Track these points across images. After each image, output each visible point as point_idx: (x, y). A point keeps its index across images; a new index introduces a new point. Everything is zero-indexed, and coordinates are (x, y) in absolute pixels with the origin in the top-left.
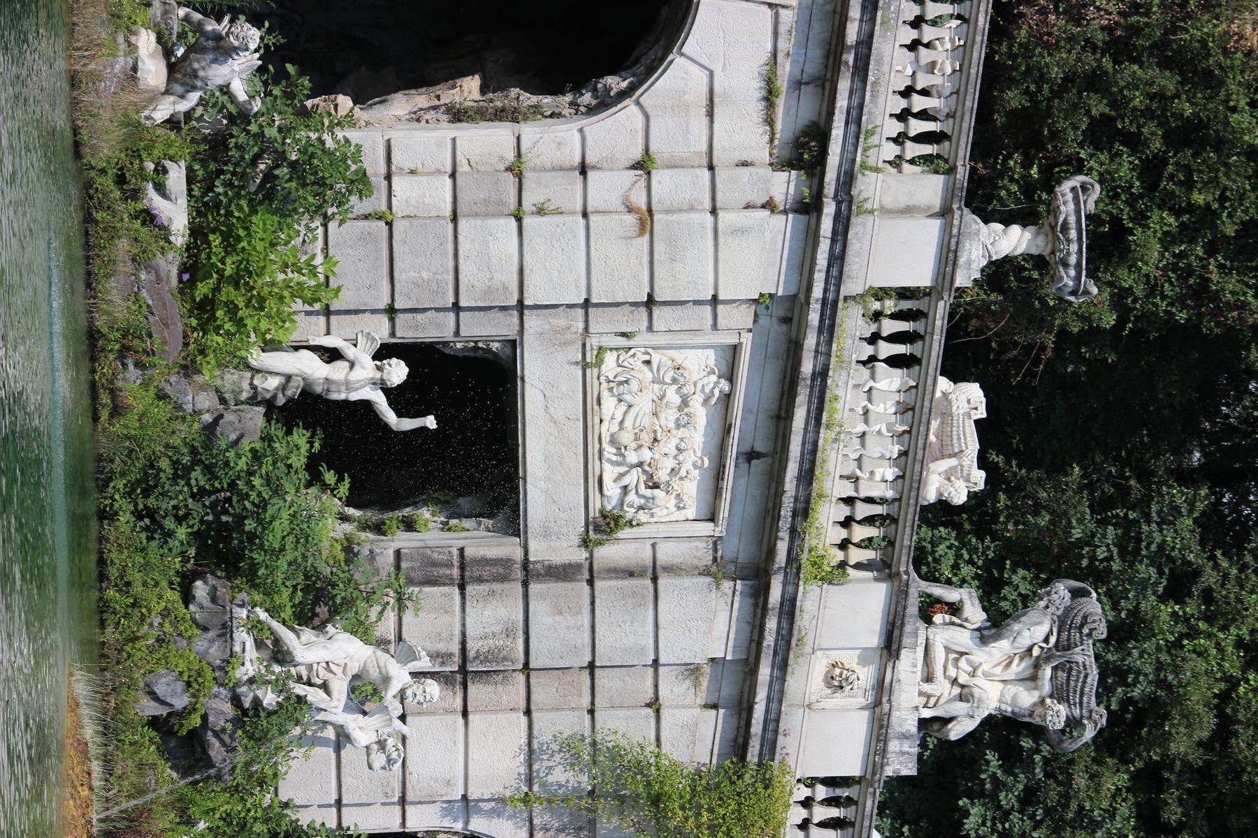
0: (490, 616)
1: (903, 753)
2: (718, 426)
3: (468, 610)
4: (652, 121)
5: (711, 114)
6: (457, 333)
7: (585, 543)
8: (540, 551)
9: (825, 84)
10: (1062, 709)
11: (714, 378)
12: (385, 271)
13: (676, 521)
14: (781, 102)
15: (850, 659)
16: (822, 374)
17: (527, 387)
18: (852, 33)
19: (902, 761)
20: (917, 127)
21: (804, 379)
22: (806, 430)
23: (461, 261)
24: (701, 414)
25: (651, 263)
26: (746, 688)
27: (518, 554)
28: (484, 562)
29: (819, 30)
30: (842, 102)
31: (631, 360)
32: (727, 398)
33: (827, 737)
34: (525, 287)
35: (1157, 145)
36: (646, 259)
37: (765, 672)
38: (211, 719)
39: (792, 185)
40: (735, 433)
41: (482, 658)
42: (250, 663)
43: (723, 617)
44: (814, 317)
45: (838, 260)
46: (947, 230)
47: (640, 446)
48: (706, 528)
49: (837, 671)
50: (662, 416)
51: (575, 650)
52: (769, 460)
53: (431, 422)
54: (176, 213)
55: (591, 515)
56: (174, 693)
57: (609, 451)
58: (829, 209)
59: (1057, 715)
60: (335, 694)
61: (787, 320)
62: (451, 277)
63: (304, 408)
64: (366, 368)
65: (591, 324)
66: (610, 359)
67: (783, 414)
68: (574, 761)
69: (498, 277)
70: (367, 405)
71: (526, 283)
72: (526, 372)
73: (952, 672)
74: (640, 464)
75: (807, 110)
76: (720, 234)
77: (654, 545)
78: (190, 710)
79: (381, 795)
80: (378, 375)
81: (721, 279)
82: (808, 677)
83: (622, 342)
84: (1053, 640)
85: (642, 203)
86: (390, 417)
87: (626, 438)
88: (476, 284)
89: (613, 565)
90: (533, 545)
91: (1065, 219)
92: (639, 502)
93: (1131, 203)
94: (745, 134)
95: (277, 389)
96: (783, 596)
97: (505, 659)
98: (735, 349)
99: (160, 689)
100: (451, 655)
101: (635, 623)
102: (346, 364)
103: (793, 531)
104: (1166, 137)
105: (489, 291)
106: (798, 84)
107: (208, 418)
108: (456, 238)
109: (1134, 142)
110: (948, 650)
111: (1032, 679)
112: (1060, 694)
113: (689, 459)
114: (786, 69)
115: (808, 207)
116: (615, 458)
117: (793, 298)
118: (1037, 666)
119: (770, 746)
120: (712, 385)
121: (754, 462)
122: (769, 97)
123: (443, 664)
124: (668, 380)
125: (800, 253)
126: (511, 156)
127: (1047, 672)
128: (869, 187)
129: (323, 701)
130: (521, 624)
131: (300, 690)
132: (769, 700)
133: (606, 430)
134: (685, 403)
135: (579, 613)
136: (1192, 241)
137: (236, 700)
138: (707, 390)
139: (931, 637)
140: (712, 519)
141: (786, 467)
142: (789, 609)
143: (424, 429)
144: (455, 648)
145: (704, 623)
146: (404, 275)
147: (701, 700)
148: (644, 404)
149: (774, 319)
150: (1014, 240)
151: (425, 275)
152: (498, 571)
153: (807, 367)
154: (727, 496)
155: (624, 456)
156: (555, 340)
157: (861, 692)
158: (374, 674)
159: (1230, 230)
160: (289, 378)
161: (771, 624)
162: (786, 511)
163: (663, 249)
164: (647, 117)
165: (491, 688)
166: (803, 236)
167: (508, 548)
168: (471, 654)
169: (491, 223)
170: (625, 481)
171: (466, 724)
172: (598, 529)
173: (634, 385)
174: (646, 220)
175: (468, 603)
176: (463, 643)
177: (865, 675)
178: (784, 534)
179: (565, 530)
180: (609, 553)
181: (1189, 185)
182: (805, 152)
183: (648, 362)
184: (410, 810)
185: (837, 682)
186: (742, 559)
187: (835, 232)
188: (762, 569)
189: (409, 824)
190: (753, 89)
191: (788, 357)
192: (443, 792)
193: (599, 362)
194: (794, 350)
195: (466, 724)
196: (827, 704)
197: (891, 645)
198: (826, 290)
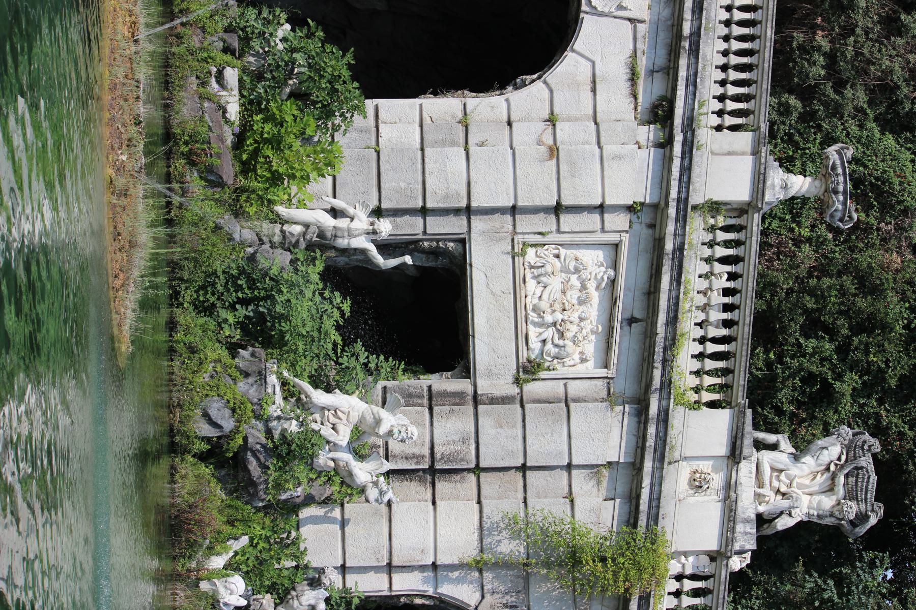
0: (451, 429)
1: (746, 533)
2: (607, 304)
3: (435, 424)
4: (555, 94)
5: (594, 90)
6: (425, 232)
7: (517, 381)
8: (485, 386)
9: (670, 71)
10: (853, 504)
11: (603, 269)
12: (375, 182)
13: (581, 359)
14: (641, 83)
15: (706, 466)
16: (680, 250)
17: (474, 269)
18: (687, 29)
19: (746, 538)
20: (731, 106)
21: (668, 254)
22: (670, 289)
23: (427, 175)
24: (595, 297)
25: (558, 179)
26: (635, 481)
27: (470, 389)
28: (445, 394)
29: (664, 37)
30: (682, 73)
31: (546, 252)
32: (613, 282)
33: (693, 526)
34: (472, 194)
35: (845, 331)
36: (554, 176)
37: (648, 465)
38: (250, 440)
39: (651, 134)
40: (620, 303)
41: (445, 459)
42: (277, 405)
43: (616, 432)
44: (672, 211)
45: (687, 169)
46: (757, 163)
47: (554, 311)
48: (603, 372)
49: (698, 475)
50: (568, 293)
51: (512, 454)
52: (644, 324)
53: (408, 259)
54: (234, 110)
55: (521, 361)
56: (223, 418)
57: (533, 316)
58: (679, 138)
59: (852, 509)
60: (341, 432)
61: (652, 226)
62: (420, 187)
63: (321, 243)
64: (362, 222)
65: (517, 226)
66: (531, 252)
67: (652, 289)
68: (515, 535)
69: (453, 186)
70: (363, 252)
71: (472, 191)
72: (473, 260)
73: (776, 484)
74: (554, 324)
75: (659, 88)
76: (605, 159)
77: (565, 385)
78: (236, 431)
79: (374, 560)
80: (371, 228)
81: (606, 190)
82: (678, 479)
83: (539, 239)
84: (844, 458)
85: (551, 142)
86: (379, 260)
87: (544, 305)
88: (438, 191)
89: (538, 397)
90: (480, 382)
91: (834, 162)
92: (554, 351)
93: (833, 368)
94: (618, 104)
95: (299, 235)
96: (659, 410)
97: (462, 460)
98: (617, 246)
99: (213, 413)
100: (423, 457)
101: (555, 435)
102: (349, 219)
103: (665, 361)
104: (850, 328)
105: (447, 197)
106: (651, 72)
107: (250, 250)
108: (423, 160)
109: (831, 332)
110: (773, 469)
111: (831, 489)
112: (851, 495)
113: (588, 326)
114: (643, 63)
115: (665, 144)
116: (536, 320)
117: (655, 207)
118: (833, 477)
119: (654, 517)
120: (602, 274)
121: (633, 325)
122: (633, 79)
123: (417, 463)
124: (572, 268)
125: (660, 174)
126: (460, 115)
127: (842, 479)
128: (704, 135)
129: (332, 435)
130: (473, 435)
131: (315, 427)
132: (652, 484)
133: (531, 302)
134: (584, 287)
135: (514, 426)
136: (869, 397)
137: (269, 432)
138: (599, 277)
139: (760, 458)
140: (606, 366)
141: (656, 323)
142: (664, 418)
143: (404, 264)
144: (427, 452)
145: (604, 436)
146: (387, 185)
147: (603, 493)
148: (555, 284)
149: (643, 225)
150: (800, 184)
151: (402, 185)
152: (457, 398)
153: (669, 246)
154: (615, 348)
155: (543, 317)
156: (493, 236)
157: (715, 492)
158: (370, 419)
159: (893, 383)
160: (307, 226)
161: (652, 430)
162: (659, 349)
163: (566, 169)
164: (551, 91)
165: (452, 485)
166: (661, 163)
167: (464, 385)
168: (438, 456)
169: (448, 150)
170: (543, 337)
171: (435, 509)
172: (526, 371)
173: (549, 268)
174: (554, 152)
175: (435, 419)
176: (432, 448)
177: (717, 480)
178: (658, 365)
179: (502, 372)
180: (533, 388)
181: (867, 353)
182: (660, 114)
183: (557, 256)
184: (395, 577)
185: (698, 484)
186: (629, 393)
187: (683, 153)
188: (643, 399)
189: (394, 588)
190: (623, 73)
191: (654, 251)
192: (419, 558)
193: (523, 254)
194: (659, 243)
195: (435, 509)
196: (692, 500)
197: (734, 455)
198: (679, 193)
